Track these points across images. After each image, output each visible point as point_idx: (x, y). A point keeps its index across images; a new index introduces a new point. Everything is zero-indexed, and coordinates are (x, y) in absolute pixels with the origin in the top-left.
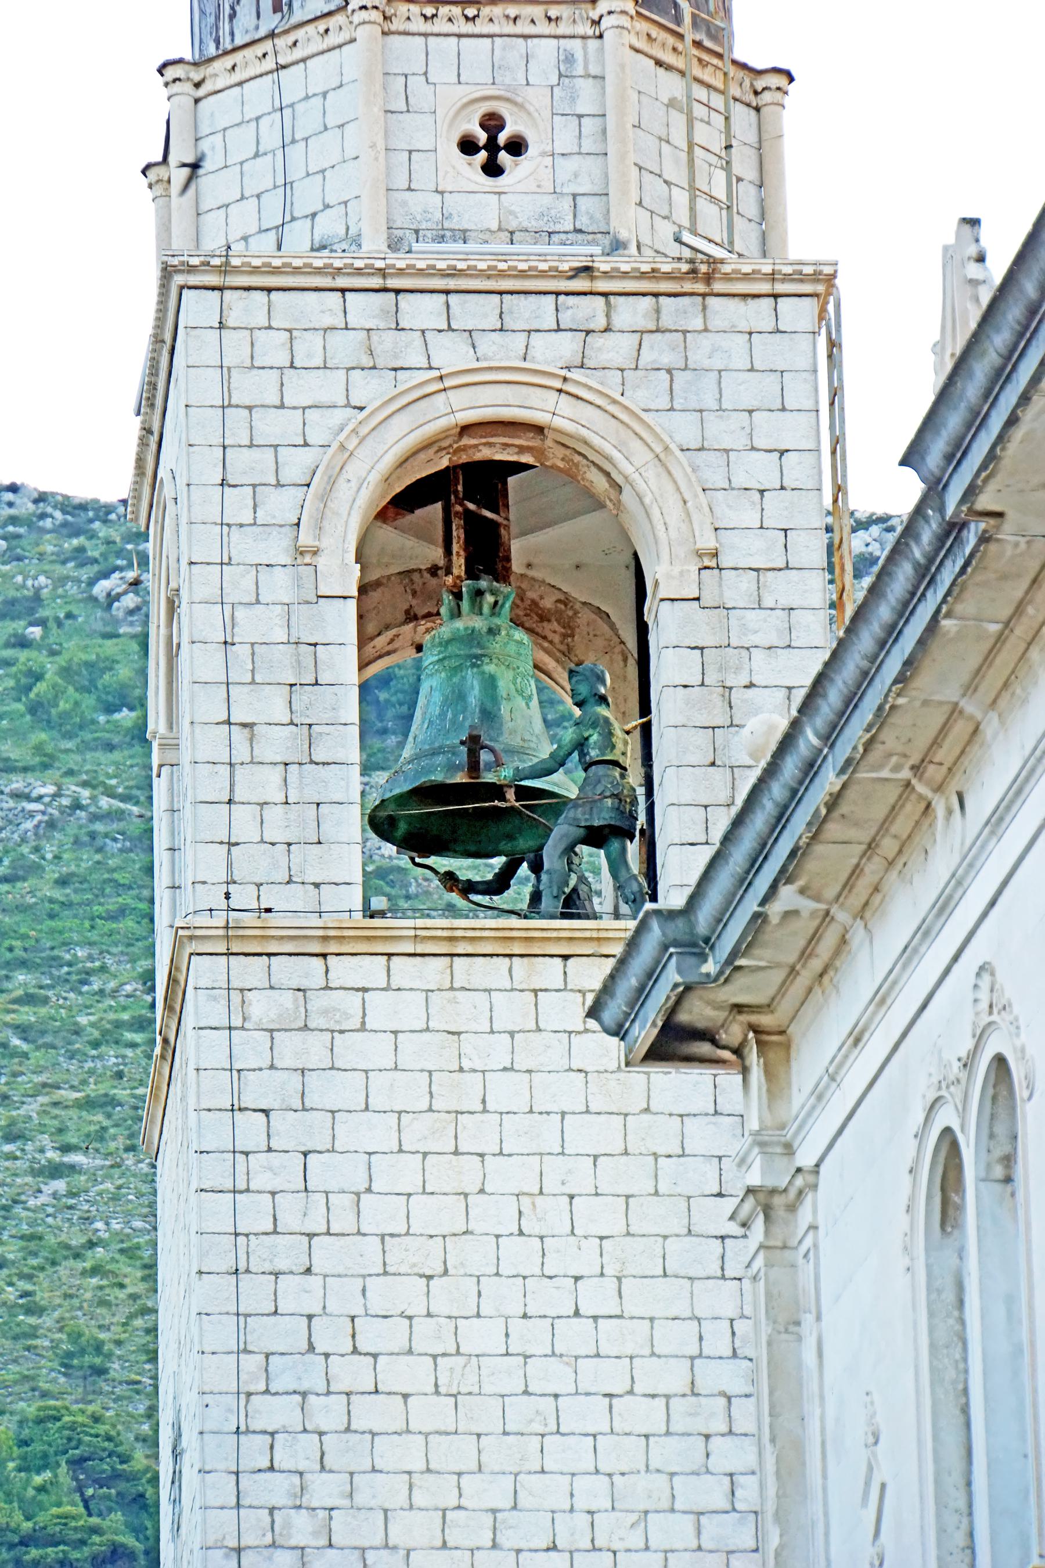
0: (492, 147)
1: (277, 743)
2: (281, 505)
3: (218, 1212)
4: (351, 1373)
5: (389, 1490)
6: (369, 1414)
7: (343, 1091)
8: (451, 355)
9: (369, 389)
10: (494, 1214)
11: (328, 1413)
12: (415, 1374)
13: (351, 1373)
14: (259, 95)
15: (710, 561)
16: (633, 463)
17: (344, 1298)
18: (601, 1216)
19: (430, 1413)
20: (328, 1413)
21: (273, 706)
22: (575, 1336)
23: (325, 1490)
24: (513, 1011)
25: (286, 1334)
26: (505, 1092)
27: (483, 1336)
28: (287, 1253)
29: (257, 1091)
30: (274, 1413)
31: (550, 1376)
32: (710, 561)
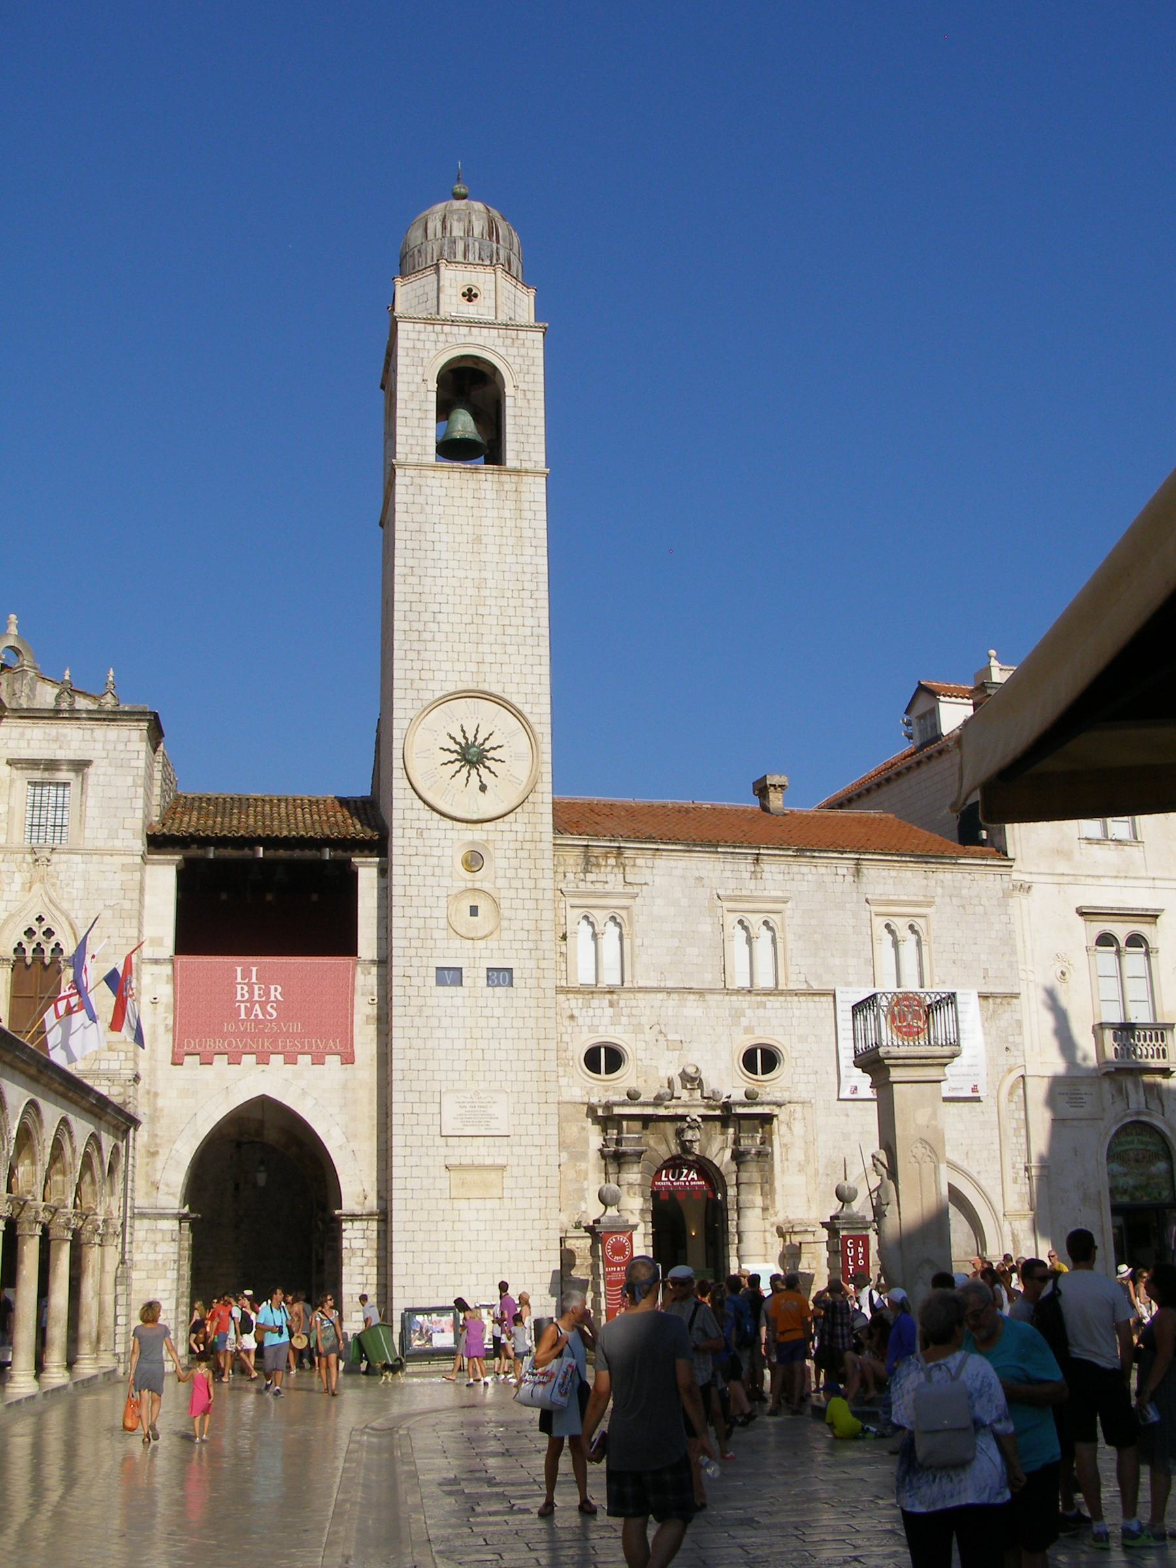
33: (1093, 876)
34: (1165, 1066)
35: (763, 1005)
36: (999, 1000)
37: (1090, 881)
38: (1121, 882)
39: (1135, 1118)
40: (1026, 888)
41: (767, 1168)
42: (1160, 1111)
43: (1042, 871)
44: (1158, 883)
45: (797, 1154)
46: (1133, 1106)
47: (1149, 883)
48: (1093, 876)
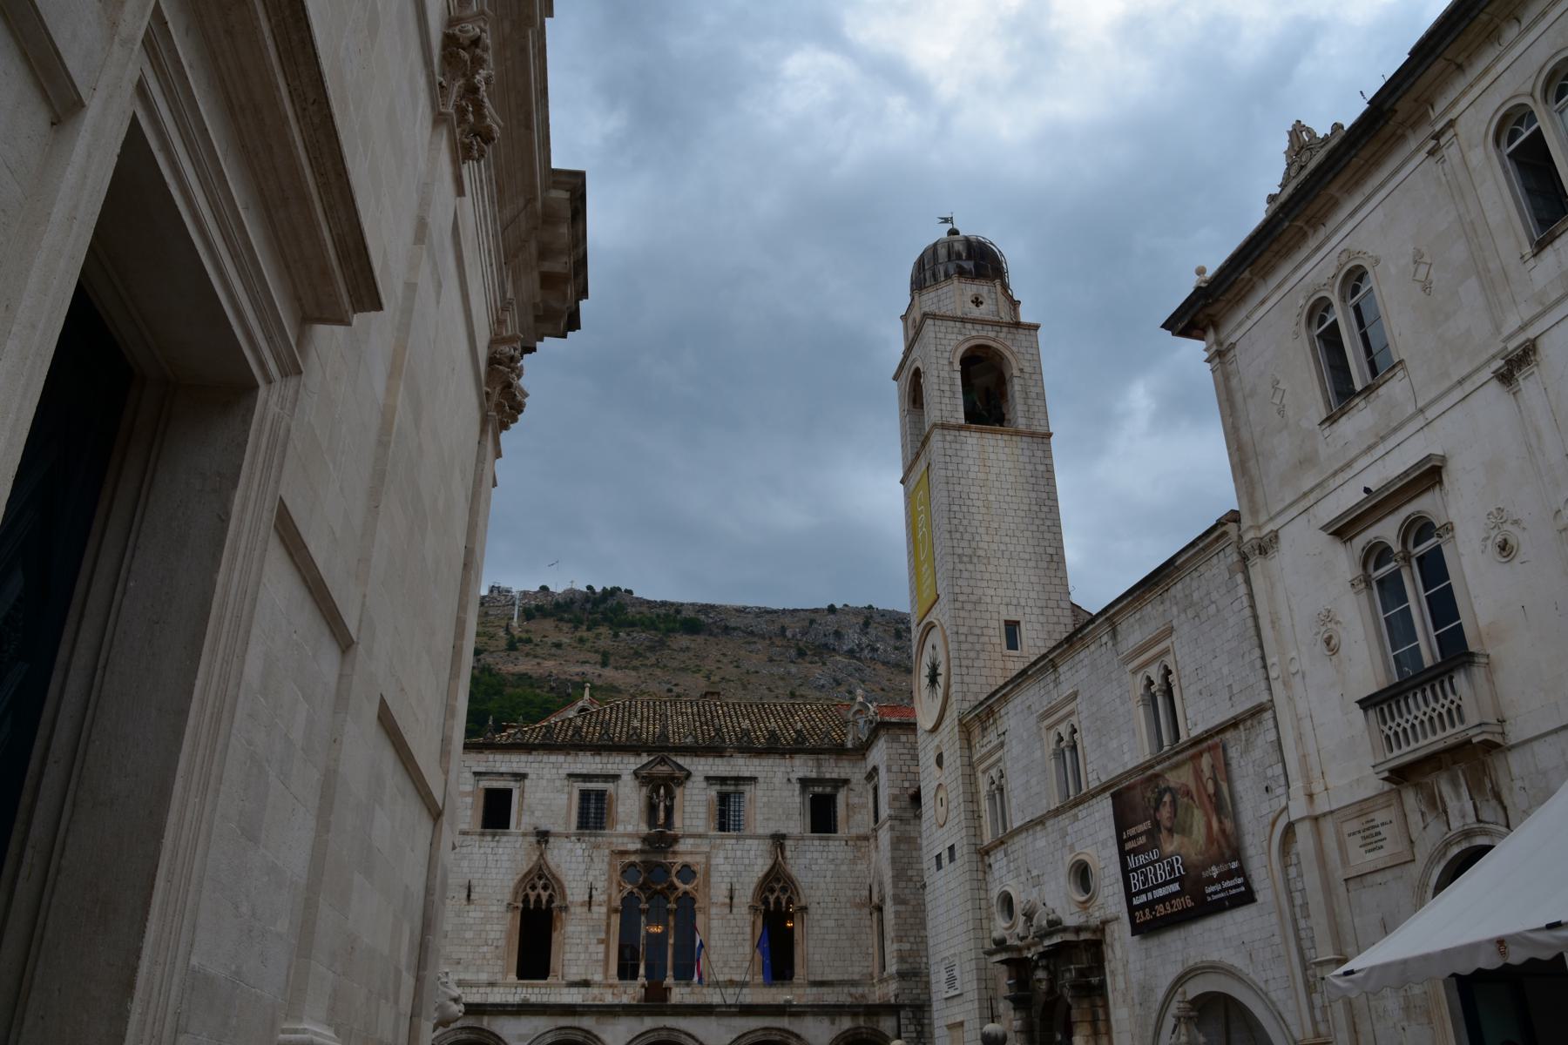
0: (977, 302)
1: (948, 394)
2: (946, 355)
3: (943, 472)
4: (968, 502)
5: (976, 523)
6: (973, 510)
7: (963, 454)
8: (974, 333)
9: (961, 338)
10: (992, 477)
11: (965, 509)
12: (979, 503)
13: (968, 502)
14: (932, 295)
15: (1021, 370)
16: (1007, 354)
17: (966, 489)
18: (1012, 479)
19: (983, 510)
20: (965, 509)
21: (946, 388)
22: (1008, 499)
23: (965, 522)
24: (992, 442)
25: (956, 495)
26: (993, 456)
27: (992, 498)
28: (955, 480)
29: (949, 452)
30: (956, 508)
31: (1005, 506)
32: (1021, 370)
33: (1342, 470)
34: (1461, 737)
35: (1076, 818)
36: (1249, 723)
37: (1339, 479)
38: (1380, 450)
39: (1465, 845)
40: (1265, 547)
41: (1099, 1002)
42: (1502, 820)
43: (1288, 502)
44: (1431, 413)
45: (1121, 984)
46: (1456, 825)
47: (1420, 421)
48: (1342, 470)
